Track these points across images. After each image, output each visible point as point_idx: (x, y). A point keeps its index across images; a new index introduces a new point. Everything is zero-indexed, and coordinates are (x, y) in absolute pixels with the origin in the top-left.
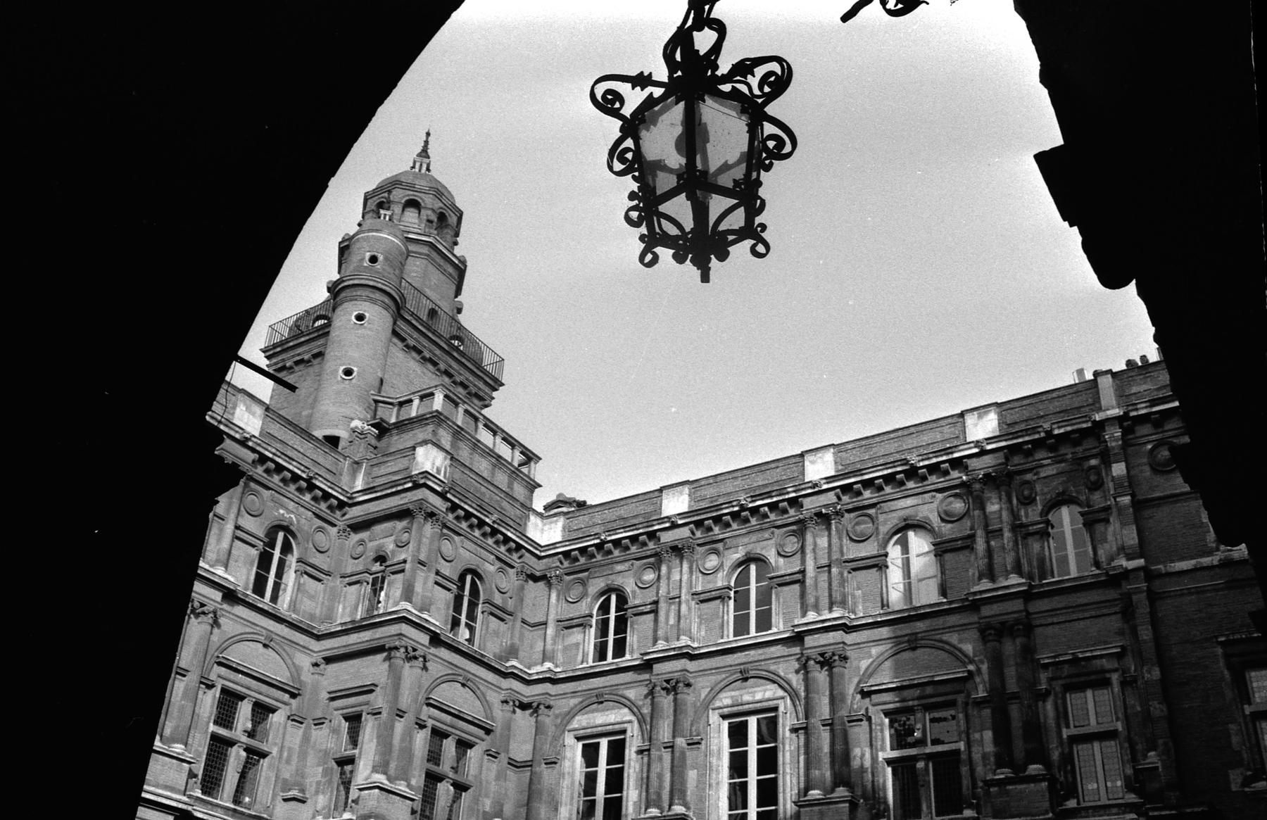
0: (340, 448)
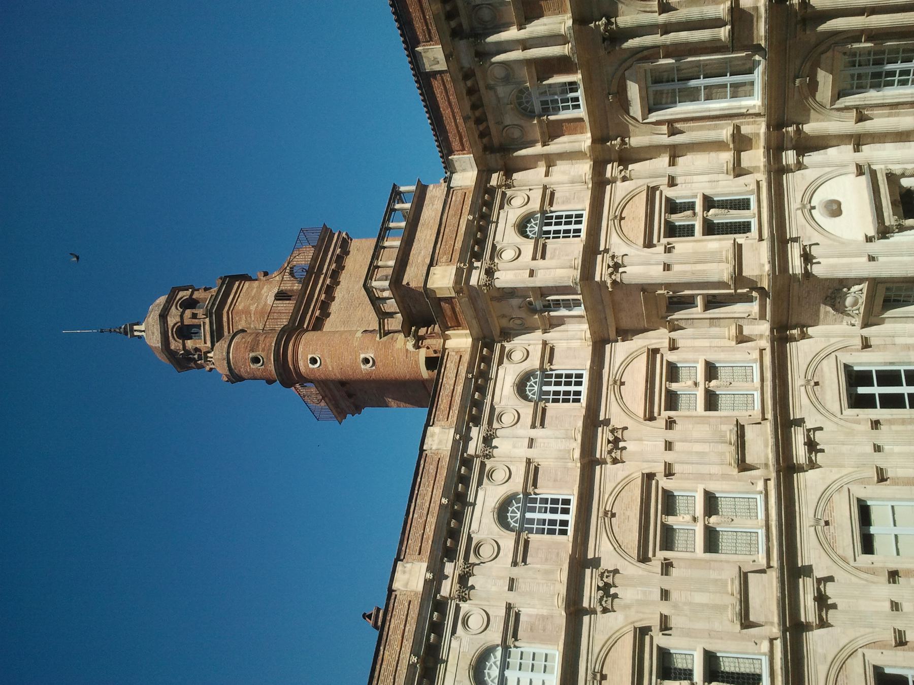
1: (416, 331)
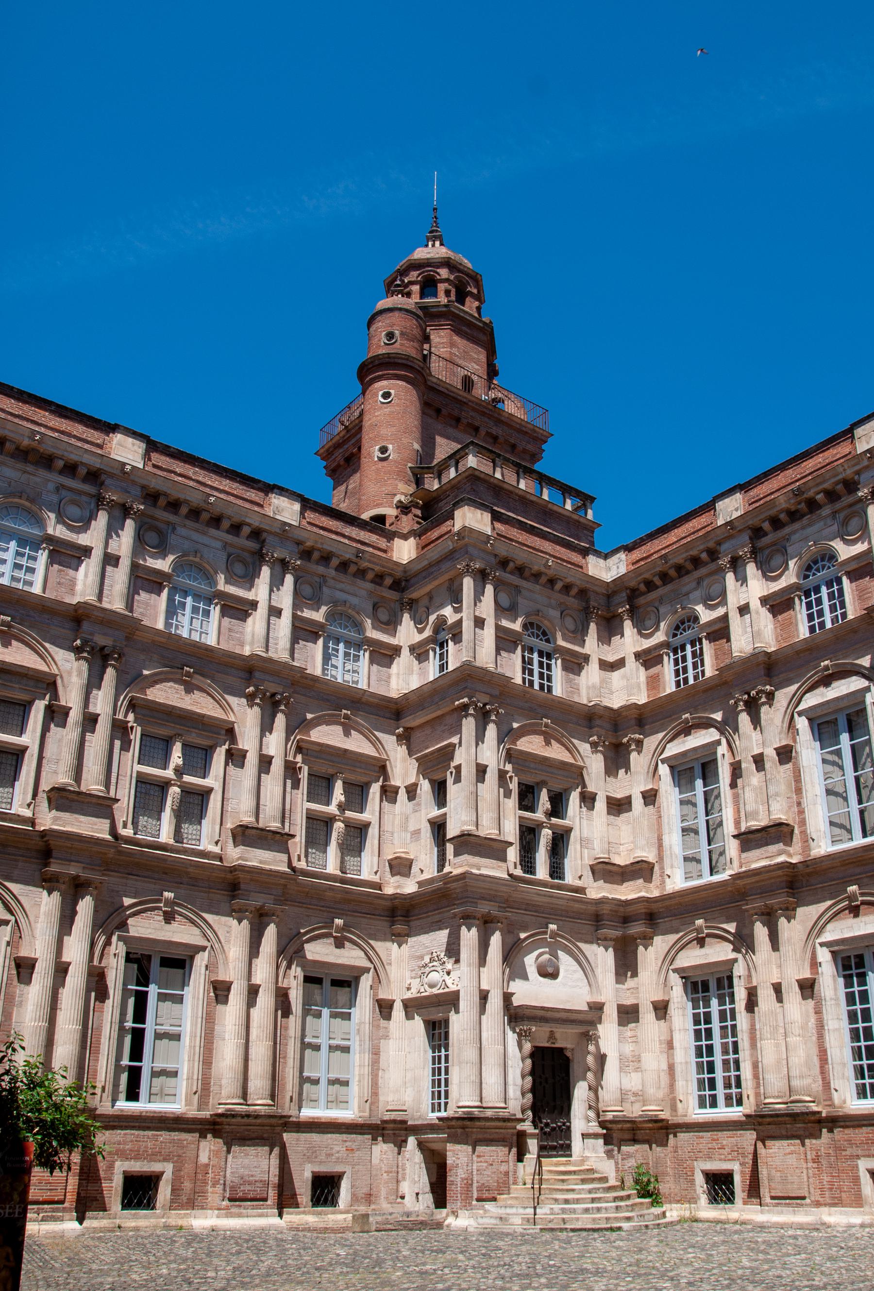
0: (387, 525)
1: (416, 506)
